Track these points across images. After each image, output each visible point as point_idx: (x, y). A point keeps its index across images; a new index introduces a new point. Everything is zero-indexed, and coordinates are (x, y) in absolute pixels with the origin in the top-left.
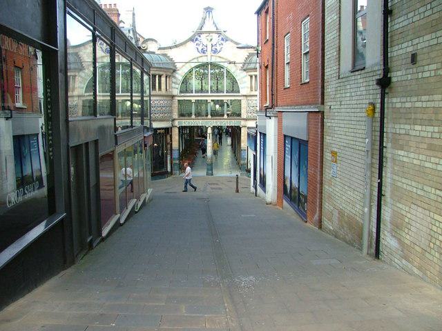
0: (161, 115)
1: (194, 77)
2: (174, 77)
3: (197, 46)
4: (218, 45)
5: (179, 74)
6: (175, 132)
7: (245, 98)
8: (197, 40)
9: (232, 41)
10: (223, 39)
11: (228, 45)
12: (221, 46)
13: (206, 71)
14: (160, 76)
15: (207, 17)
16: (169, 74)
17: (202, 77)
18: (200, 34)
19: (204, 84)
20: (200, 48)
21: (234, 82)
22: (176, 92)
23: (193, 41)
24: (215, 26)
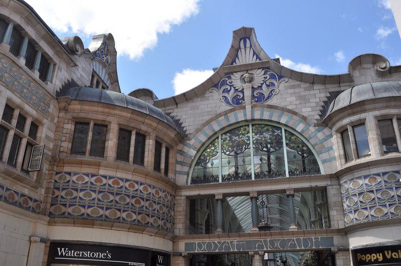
0: (134, 217)
1: (219, 150)
2: (181, 152)
3: (226, 95)
4: (264, 86)
7: (335, 182)
8: (224, 83)
10: (272, 77)
11: (282, 86)
12: (271, 88)
13: (245, 138)
14: (142, 137)
16: (166, 139)
17: (238, 150)
18: (229, 74)
20: (230, 96)
22: (181, 180)
23: (216, 86)
24: (258, 57)
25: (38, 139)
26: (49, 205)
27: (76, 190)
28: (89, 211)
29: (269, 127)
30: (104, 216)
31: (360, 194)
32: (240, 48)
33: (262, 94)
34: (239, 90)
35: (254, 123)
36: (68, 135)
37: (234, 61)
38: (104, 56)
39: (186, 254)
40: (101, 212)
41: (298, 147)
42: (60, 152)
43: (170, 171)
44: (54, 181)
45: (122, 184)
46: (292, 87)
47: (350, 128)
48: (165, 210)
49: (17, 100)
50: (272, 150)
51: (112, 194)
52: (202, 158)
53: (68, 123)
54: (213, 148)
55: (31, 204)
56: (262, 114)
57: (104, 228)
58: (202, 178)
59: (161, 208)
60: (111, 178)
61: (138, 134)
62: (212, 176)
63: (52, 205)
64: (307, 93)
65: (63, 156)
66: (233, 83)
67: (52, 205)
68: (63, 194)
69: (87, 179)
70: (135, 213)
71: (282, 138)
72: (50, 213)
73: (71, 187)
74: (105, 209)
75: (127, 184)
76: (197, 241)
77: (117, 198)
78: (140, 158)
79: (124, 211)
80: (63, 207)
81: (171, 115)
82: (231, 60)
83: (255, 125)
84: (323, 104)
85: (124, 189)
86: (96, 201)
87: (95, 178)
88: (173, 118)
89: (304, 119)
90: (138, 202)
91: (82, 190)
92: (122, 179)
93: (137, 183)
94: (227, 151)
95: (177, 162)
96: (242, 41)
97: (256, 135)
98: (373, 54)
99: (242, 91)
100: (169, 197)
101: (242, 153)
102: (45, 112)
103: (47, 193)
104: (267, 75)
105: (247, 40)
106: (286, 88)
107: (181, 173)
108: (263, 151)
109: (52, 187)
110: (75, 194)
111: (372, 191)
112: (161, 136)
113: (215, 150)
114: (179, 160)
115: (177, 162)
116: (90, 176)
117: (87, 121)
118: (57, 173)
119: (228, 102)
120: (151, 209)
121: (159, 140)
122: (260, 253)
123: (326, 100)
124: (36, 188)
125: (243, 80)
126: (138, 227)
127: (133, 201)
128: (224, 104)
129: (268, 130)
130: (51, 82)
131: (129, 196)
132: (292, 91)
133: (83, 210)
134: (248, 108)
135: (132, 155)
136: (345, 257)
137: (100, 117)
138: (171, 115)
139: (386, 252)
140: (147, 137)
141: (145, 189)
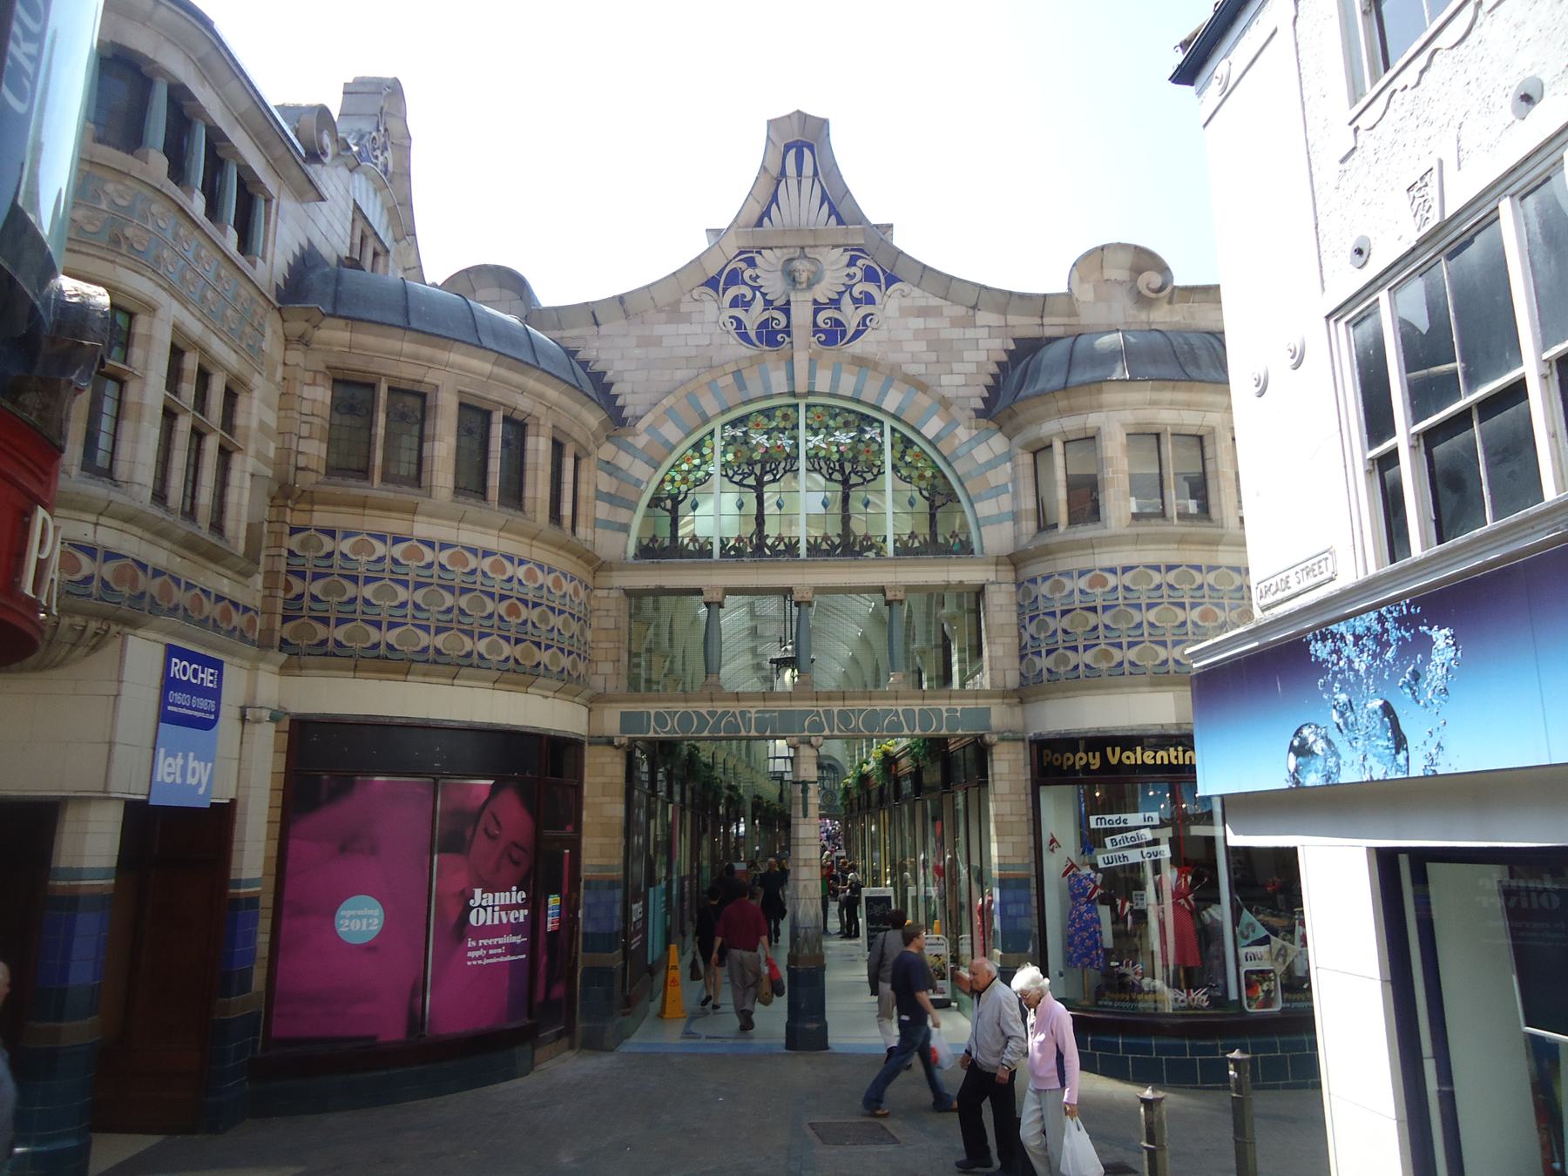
0: (507, 650)
1: (714, 469)
2: (610, 468)
3: (739, 312)
4: (846, 298)
5: (631, 450)
6: (602, 777)
8: (734, 278)
9: (925, 274)
10: (870, 275)
13: (785, 442)
14: (517, 428)
15: (791, 169)
16: (576, 433)
19: (770, 508)
20: (753, 318)
21: (939, 496)
23: (712, 283)
24: (833, 211)
25: (238, 432)
26: (279, 619)
27: (354, 579)
28: (392, 636)
29: (851, 417)
30: (431, 650)
31: (1064, 613)
32: (783, 173)
33: (838, 323)
34: (776, 304)
35: (811, 400)
36: (316, 420)
37: (767, 213)
38: (378, 152)
39: (624, 741)
40: (425, 639)
41: (922, 477)
42: (297, 468)
43: (581, 520)
44: (285, 553)
45: (473, 562)
46: (923, 312)
47: (1058, 446)
48: (575, 627)
49: (194, 327)
50: (854, 479)
51: (450, 589)
52: (668, 487)
53: (314, 384)
54: (697, 462)
55: (238, 619)
56: (835, 380)
57: (434, 680)
58: (667, 543)
59: (565, 623)
60: (444, 546)
61: (506, 419)
62: (694, 539)
63: (286, 619)
64: (956, 333)
65: (306, 481)
66: (760, 282)
67: (286, 619)
68: (316, 588)
69: (380, 549)
70: (507, 639)
71: (881, 451)
72: (283, 641)
73: (336, 570)
74: (433, 631)
75: (486, 564)
76: (652, 708)
77: (463, 602)
78: (514, 494)
79: (482, 636)
80: (319, 627)
81: (580, 356)
82: (757, 210)
83: (815, 406)
84: (994, 369)
85: (479, 577)
86: (410, 609)
87: (404, 545)
88: (584, 364)
89: (945, 403)
90: (513, 611)
91: (368, 580)
92: (474, 551)
93: (511, 559)
94: (735, 473)
95: (600, 495)
96: (792, 152)
97: (816, 434)
98: (1136, 247)
99: (786, 309)
100: (582, 593)
101: (774, 481)
102: (254, 353)
103: (270, 585)
104: (853, 270)
105: (806, 152)
106: (905, 312)
107: (608, 525)
108: (830, 479)
109: (283, 568)
110: (351, 590)
111: (1094, 609)
112: (565, 424)
113: (704, 467)
114: (603, 488)
115: (600, 495)
116: (389, 542)
117: (369, 379)
118: (294, 531)
119: (744, 337)
120: (543, 627)
121: (560, 438)
122: (813, 740)
123: (1004, 358)
124: (247, 574)
125: (791, 277)
126: (517, 675)
127: (502, 608)
128: (733, 339)
129: (846, 424)
130: (264, 258)
131: (491, 595)
132: (918, 323)
133: (375, 635)
134: (801, 360)
135: (494, 481)
136: (1012, 757)
137: (408, 372)
138: (580, 356)
139: (1109, 750)
140: (531, 430)
141: (530, 575)
